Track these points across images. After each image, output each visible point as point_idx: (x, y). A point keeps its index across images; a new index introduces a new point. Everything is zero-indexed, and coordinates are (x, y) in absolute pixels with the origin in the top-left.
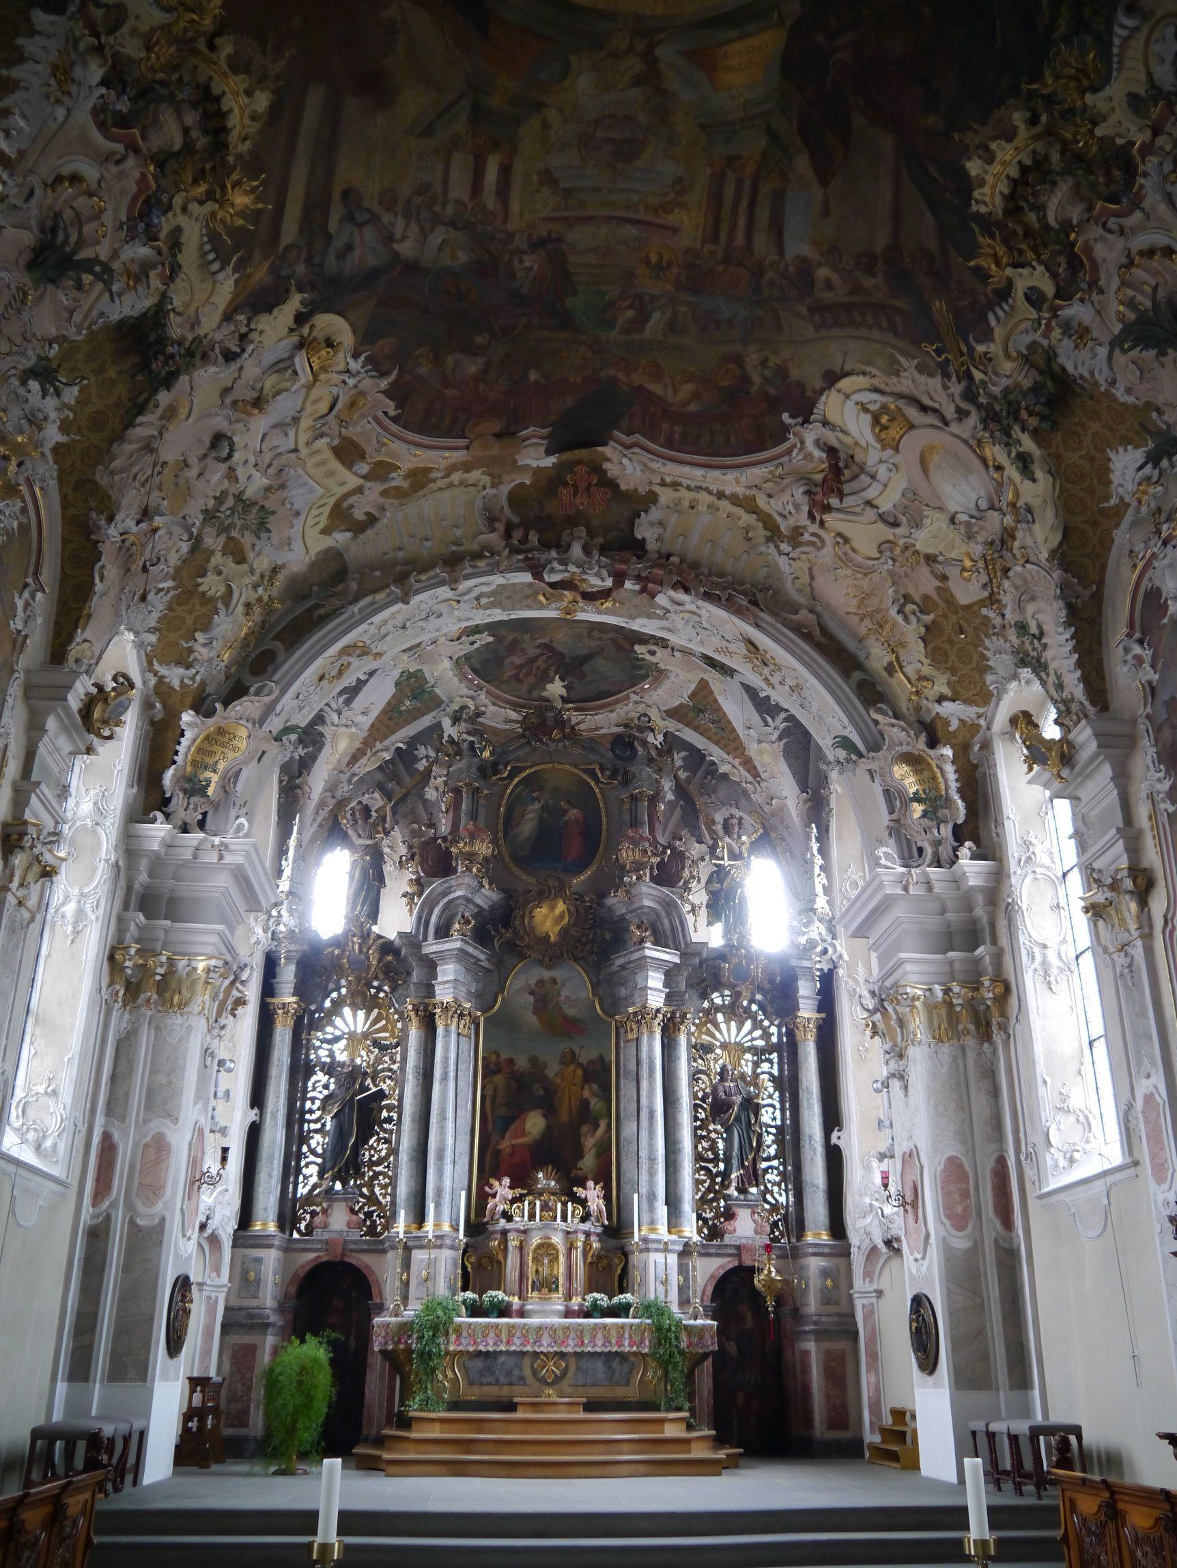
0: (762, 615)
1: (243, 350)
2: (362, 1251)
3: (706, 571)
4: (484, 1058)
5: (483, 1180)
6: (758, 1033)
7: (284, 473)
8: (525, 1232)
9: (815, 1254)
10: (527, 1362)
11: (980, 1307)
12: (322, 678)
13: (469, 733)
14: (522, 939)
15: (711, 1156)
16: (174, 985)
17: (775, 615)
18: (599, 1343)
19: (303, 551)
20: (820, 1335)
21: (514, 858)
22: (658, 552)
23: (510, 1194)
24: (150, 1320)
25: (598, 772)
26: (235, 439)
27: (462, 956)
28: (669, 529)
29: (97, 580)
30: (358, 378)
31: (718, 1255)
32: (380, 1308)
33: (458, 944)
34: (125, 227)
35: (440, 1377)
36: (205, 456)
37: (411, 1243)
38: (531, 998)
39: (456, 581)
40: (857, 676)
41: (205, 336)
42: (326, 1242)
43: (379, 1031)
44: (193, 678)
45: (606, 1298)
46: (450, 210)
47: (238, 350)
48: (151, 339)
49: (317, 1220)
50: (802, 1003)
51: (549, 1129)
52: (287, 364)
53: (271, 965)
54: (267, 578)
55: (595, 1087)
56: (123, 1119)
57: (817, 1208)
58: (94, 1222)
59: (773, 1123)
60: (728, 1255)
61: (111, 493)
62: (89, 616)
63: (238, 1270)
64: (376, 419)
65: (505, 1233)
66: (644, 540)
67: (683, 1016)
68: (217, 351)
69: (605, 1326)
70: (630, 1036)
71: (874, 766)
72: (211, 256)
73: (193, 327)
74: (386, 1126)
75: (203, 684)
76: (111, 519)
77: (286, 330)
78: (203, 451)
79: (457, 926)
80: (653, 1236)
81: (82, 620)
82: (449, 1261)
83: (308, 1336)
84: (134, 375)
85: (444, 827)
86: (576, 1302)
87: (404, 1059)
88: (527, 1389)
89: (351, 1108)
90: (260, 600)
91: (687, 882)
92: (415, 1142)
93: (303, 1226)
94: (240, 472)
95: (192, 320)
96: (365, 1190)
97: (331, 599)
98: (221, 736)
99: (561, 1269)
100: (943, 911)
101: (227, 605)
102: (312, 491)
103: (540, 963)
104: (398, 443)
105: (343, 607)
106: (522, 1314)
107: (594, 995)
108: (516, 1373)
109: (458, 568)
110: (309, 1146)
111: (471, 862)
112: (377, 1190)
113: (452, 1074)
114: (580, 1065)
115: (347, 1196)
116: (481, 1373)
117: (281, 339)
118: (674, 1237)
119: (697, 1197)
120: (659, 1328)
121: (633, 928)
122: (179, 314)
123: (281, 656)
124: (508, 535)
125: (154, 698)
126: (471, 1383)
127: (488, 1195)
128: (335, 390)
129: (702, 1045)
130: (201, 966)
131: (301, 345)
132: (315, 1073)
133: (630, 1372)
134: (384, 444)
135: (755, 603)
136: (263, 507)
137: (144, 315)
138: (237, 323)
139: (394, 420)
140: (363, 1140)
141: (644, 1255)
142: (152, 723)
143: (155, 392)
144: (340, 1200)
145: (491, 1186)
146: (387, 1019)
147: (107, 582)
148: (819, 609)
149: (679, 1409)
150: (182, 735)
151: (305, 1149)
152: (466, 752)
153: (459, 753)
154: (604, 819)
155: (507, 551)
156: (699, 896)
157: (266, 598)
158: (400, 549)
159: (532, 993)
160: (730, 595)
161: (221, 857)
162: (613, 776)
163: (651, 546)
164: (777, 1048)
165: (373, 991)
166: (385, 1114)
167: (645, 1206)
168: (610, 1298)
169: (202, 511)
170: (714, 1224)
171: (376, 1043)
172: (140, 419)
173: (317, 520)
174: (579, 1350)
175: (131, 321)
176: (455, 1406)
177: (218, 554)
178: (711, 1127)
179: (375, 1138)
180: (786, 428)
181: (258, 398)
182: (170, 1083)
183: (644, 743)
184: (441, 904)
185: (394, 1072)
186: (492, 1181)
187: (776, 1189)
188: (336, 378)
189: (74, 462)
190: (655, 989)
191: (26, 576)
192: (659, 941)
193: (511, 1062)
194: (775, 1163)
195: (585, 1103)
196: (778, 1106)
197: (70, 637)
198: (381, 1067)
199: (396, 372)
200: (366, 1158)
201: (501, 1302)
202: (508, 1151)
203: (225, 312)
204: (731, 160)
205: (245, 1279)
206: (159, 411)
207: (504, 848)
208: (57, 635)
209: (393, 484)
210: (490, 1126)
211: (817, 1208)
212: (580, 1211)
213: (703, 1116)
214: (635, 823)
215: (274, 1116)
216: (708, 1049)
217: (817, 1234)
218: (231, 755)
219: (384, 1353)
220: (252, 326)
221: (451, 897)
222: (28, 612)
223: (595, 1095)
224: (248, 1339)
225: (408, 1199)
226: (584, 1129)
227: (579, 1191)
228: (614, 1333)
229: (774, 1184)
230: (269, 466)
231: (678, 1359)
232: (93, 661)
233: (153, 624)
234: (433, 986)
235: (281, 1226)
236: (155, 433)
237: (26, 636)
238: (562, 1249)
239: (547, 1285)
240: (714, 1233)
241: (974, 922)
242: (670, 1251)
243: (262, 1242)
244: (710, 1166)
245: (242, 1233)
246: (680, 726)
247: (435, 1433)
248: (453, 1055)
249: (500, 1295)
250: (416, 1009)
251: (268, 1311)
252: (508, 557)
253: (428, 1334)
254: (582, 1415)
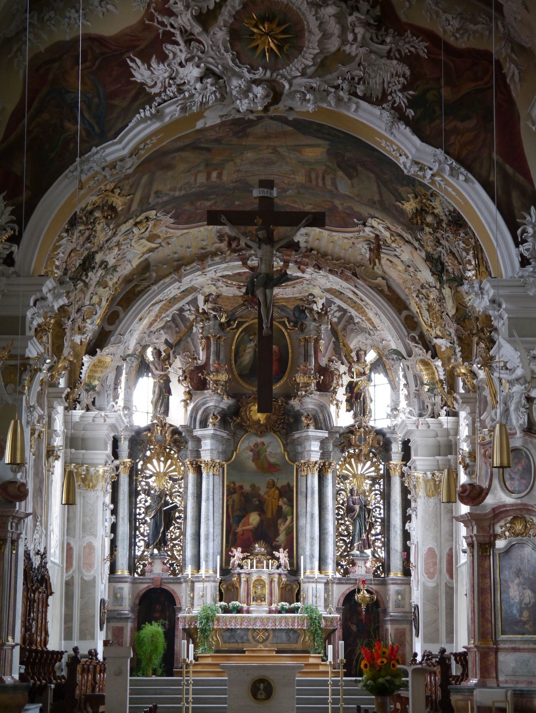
0: (359, 281)
2: (170, 583)
3: (330, 257)
4: (227, 486)
5: (228, 550)
6: (373, 469)
8: (249, 574)
9: (393, 584)
10: (250, 633)
11: (437, 611)
13: (213, 309)
14: (246, 422)
15: (346, 533)
16: (89, 478)
17: (365, 280)
18: (283, 624)
20: (393, 621)
21: (240, 375)
22: (306, 247)
23: (241, 556)
24: (94, 616)
25: (287, 323)
27: (214, 436)
28: (311, 237)
31: (346, 583)
32: (180, 609)
33: (212, 432)
35: (211, 640)
37: (194, 580)
38: (251, 454)
39: (204, 269)
40: (405, 313)
42: (152, 579)
43: (172, 471)
44: (86, 338)
45: (288, 604)
46: (197, 185)
49: (147, 568)
50: (393, 456)
51: (261, 522)
53: (116, 442)
55: (285, 499)
56: (74, 537)
57: (396, 563)
58: (67, 579)
59: (379, 516)
60: (352, 584)
63: (112, 593)
64: (166, 227)
65: (239, 574)
66: (299, 242)
67: (330, 464)
69: (286, 617)
70: (303, 474)
71: (409, 363)
74: (178, 521)
76: (69, 318)
79: (211, 420)
80: (311, 576)
82: (213, 588)
83: (153, 622)
85: (202, 356)
86: (274, 606)
87: (186, 488)
88: (250, 645)
89: (161, 513)
91: (335, 388)
92: (193, 531)
93: (139, 570)
96: (169, 553)
97: (143, 282)
98: (100, 364)
99: (267, 591)
100: (437, 436)
103: (256, 435)
105: (149, 286)
106: (248, 612)
107: (285, 451)
108: (245, 638)
109: (205, 262)
110: (140, 532)
111: (217, 385)
112: (175, 553)
113: (211, 497)
114: (277, 488)
115: (161, 557)
116: (229, 638)
118: (322, 576)
119: (338, 554)
120: (311, 618)
121: (303, 419)
123: (121, 315)
124: (230, 245)
126: (225, 642)
127: (231, 556)
129: (343, 476)
130: (101, 471)
132: (140, 494)
133: (298, 638)
135: (355, 274)
140: (167, 528)
141: (307, 585)
144: (158, 559)
145: (232, 552)
146: (176, 465)
148: (387, 277)
149: (319, 653)
150: (83, 365)
151: (138, 533)
152: (212, 319)
153: (208, 319)
154: (290, 351)
155: (229, 252)
156: (341, 395)
158: (175, 253)
159: (252, 450)
160: (342, 270)
161: (105, 421)
162: (295, 326)
163: (302, 245)
164: (382, 476)
165: (168, 450)
166: (177, 514)
167: (308, 560)
168: (290, 604)
170: (347, 568)
171: (171, 478)
174: (274, 628)
176: (217, 651)
178: (346, 519)
179: (172, 527)
180: (357, 225)
182: (92, 520)
183: (311, 310)
184: (202, 409)
185: (181, 493)
186: (233, 549)
187: (379, 550)
190: (315, 451)
192: (317, 427)
193: (241, 487)
194: (380, 537)
195: (280, 508)
196: (382, 507)
198: (174, 490)
200: (169, 537)
201: (238, 607)
202: (241, 533)
204: (312, 169)
205: (116, 596)
207: (235, 370)
210: (231, 521)
211: (396, 563)
212: (276, 563)
213: (342, 513)
214: (307, 357)
215: (123, 519)
216: (345, 477)
217: (396, 573)
218: (104, 370)
219: (184, 629)
221: (207, 405)
223: (285, 504)
224: (120, 624)
225: (192, 558)
226: (280, 521)
227: (276, 554)
228: (290, 620)
229: (379, 548)
231: (319, 631)
234: (199, 451)
235: (130, 572)
238: (267, 582)
239: (260, 598)
240: (346, 572)
241: (451, 441)
242: (320, 582)
243: (121, 580)
244: (345, 538)
245: (112, 576)
246: (333, 297)
247: (209, 661)
248: (211, 487)
249: (237, 603)
250: (192, 464)
251: (127, 612)
252: (230, 255)
253: (204, 621)
254: (274, 654)
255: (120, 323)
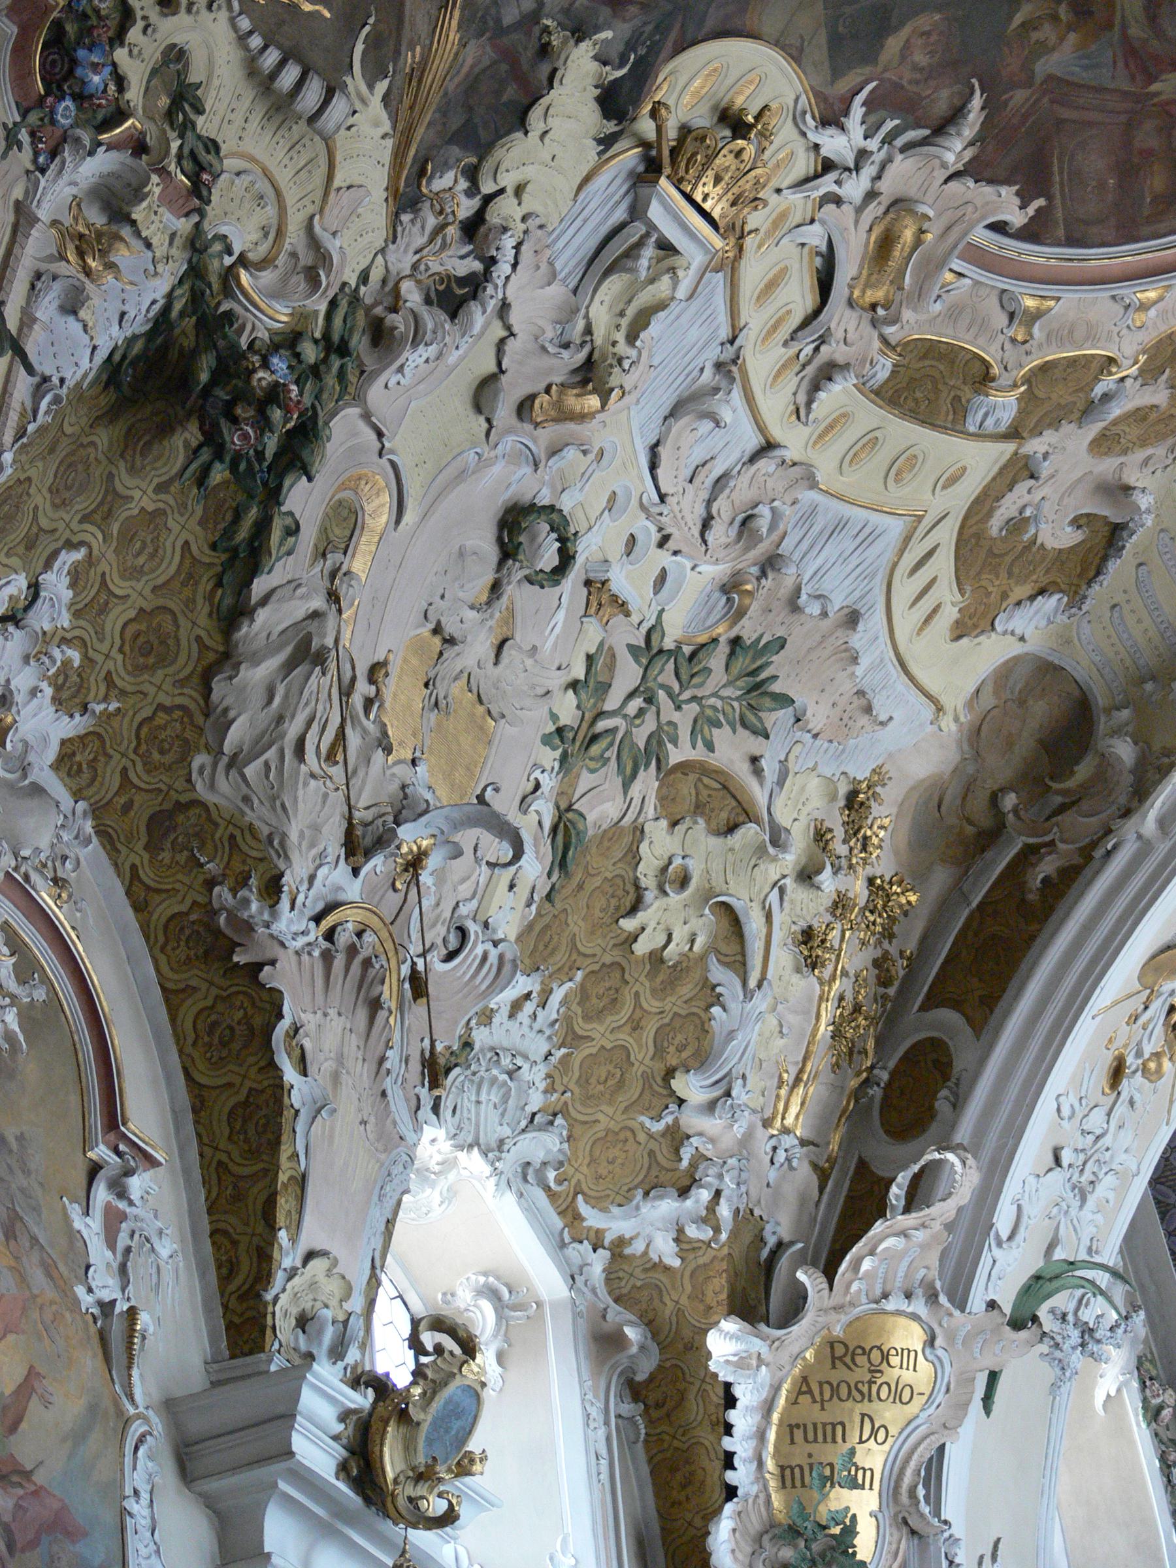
1: (493, 261)
7: (763, 524)
12: (1117, 1073)
19: (928, 711)
26: (566, 503)
29: (290, 1074)
30: (869, 171)
34: (24, 136)
36: (496, 588)
41: (364, 278)
44: (710, 1217)
47: (477, 266)
48: (204, 377)
52: (639, 228)
54: (839, 832)
61: (250, 816)
62: (301, 1181)
64: (978, 257)
68: (412, 294)
72: (290, 75)
73: (314, 282)
75: (746, 1218)
76: (273, 889)
77: (592, 150)
78: (489, 578)
81: (284, 1204)
84: (202, 478)
90: (840, 905)
94: (621, 581)
95: (306, 259)
97: (1067, 818)
101: (740, 965)
102: (867, 537)
104: (1071, 297)
105: (1109, 832)
117: (587, 180)
122: (265, 263)
123: (962, 1061)
125: (616, 1314)
128: (815, 236)
131: (651, 168)
134: (1034, 317)
136: (736, 642)
137: (162, 321)
138: (439, 203)
139: (1031, 233)
142: (634, 1390)
143: (274, 495)
147: (322, 1063)
150: (730, 1401)
157: (859, 890)
169: (546, 740)
172: (259, 586)
173: (926, 604)
175: (138, 347)
177: (657, 830)
181: (589, 362)
188: (797, 202)
189: (124, 771)
191: (86, 1144)
197: (264, 1258)
199: (977, 102)
203: (393, 190)
206: (308, 536)
208: (227, 1270)
209: (1116, 410)
218: (890, 1415)
220: (487, 188)
222: (123, 1240)
230: (706, 524)
232: (356, 1304)
233: (536, 1101)
236: (318, 602)
237: (132, 1313)
255: (958, 1105)
